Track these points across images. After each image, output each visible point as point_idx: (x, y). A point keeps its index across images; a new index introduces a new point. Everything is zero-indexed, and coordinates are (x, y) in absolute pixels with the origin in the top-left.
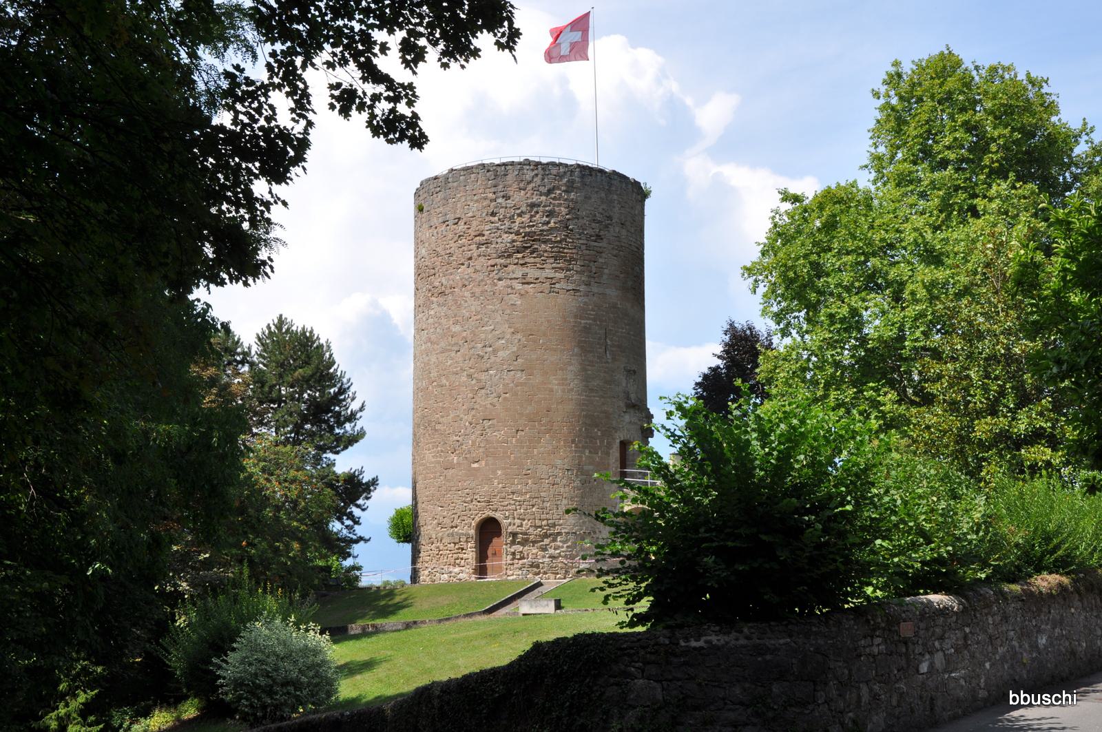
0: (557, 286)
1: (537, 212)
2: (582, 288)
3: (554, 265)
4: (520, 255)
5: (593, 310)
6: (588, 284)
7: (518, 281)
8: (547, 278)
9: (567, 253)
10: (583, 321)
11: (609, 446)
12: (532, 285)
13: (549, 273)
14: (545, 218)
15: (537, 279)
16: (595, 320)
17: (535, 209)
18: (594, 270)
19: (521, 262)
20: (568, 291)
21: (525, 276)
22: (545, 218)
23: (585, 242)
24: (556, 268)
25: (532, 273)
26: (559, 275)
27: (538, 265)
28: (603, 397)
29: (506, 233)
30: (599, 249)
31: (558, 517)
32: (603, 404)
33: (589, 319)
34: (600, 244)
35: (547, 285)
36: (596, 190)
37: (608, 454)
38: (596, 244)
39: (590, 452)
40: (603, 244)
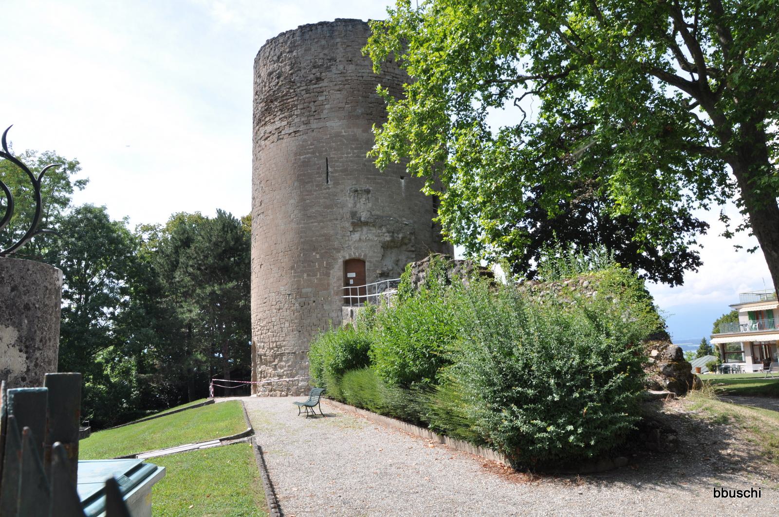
0: (283, 133)
3: (281, 116)
5: (312, 144)
6: (307, 123)
9: (289, 103)
10: (302, 157)
11: (330, 267)
12: (269, 139)
13: (278, 124)
14: (277, 81)
16: (313, 153)
18: (313, 110)
20: (290, 134)
23: (304, 88)
26: (284, 123)
27: (272, 121)
28: (323, 222)
30: (318, 89)
31: (283, 339)
32: (322, 228)
33: (308, 153)
34: (320, 85)
36: (316, 40)
37: (328, 275)
38: (315, 86)
39: (308, 275)
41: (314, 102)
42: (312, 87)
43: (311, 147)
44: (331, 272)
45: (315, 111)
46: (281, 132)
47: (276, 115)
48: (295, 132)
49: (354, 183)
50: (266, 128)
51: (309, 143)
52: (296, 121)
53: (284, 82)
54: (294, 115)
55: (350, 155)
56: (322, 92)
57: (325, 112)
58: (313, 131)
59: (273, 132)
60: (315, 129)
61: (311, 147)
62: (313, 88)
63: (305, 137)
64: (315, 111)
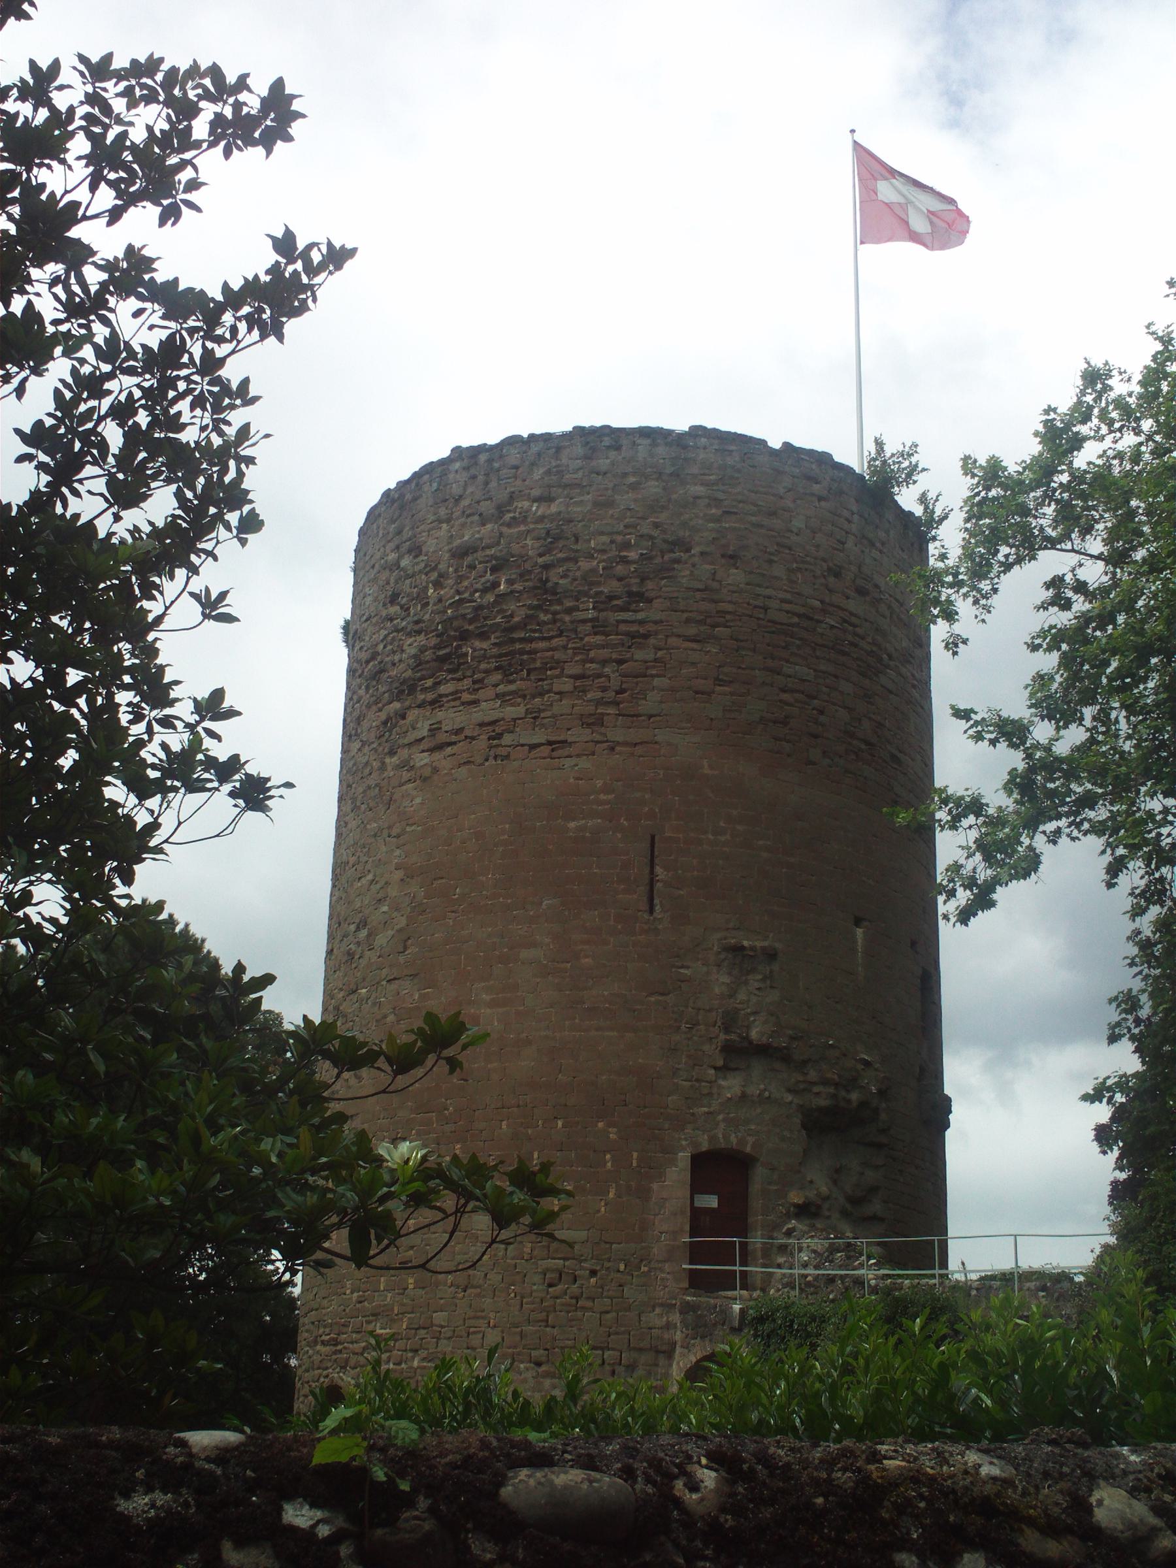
0: (507, 739)
1: (472, 567)
2: (580, 735)
4: (429, 683)
6: (594, 722)
7: (422, 747)
8: (481, 725)
10: (572, 825)
12: (449, 750)
13: (488, 710)
14: (489, 576)
15: (462, 729)
17: (468, 560)
18: (615, 683)
19: (430, 696)
20: (533, 747)
21: (434, 731)
22: (489, 576)
24: (504, 694)
25: (451, 718)
26: (511, 712)
27: (466, 697)
29: (409, 635)
30: (634, 628)
34: (640, 616)
35: (482, 743)
40: (653, 612)
41: (620, 662)
42: (614, 617)
43: (602, 797)
44: (655, 1186)
45: (621, 691)
46: (499, 736)
47: (481, 681)
48: (550, 743)
49: (731, 925)
50: (440, 715)
51: (599, 783)
52: (556, 709)
53: (518, 587)
54: (549, 691)
55: (723, 838)
56: (646, 636)
57: (654, 696)
58: (612, 749)
59: (468, 733)
60: (618, 743)
61: (602, 797)
62: (618, 622)
63: (584, 763)
64: (621, 691)
